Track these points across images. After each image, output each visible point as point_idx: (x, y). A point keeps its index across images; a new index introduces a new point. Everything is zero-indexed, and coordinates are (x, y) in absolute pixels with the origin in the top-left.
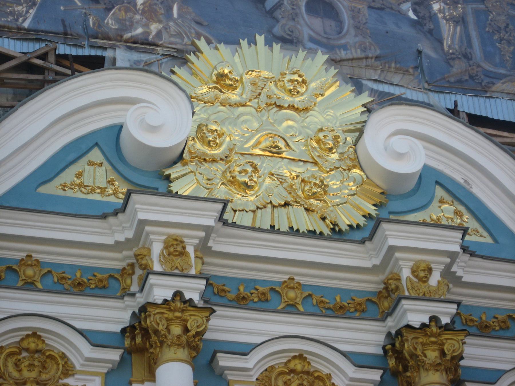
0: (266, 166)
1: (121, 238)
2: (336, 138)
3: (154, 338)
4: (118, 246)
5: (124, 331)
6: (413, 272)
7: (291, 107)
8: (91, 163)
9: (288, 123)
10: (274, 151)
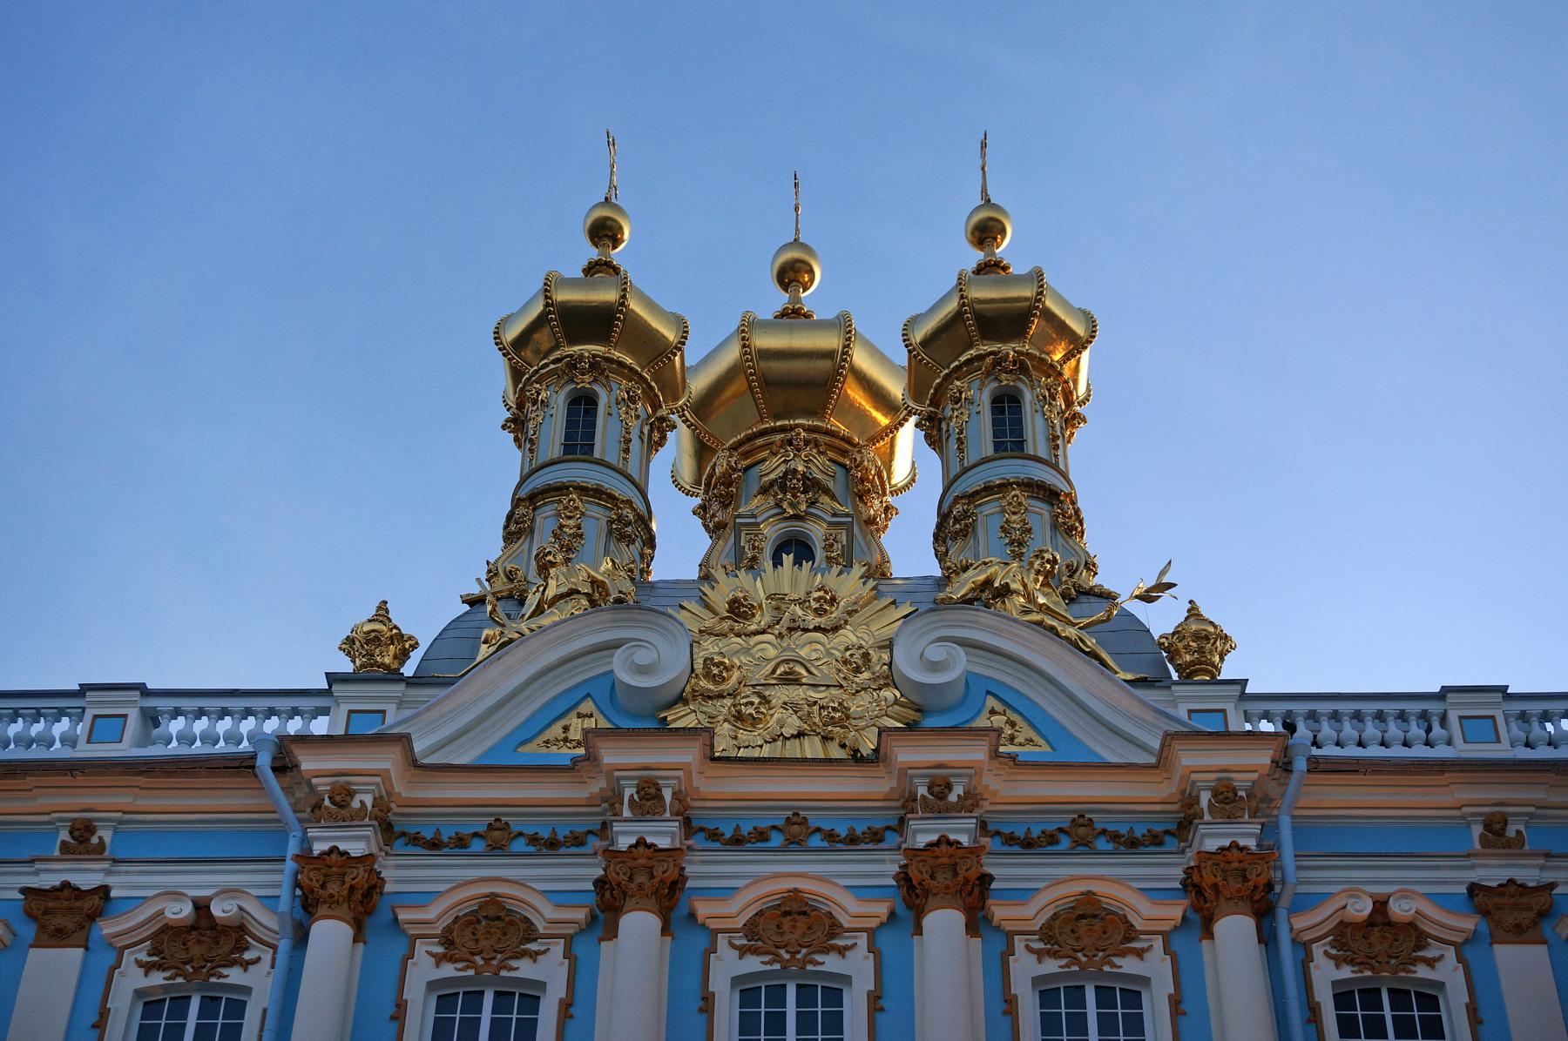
0: (780, 694)
2: (866, 656)
6: (930, 789)
7: (817, 629)
8: (580, 716)
9: (808, 648)
10: (790, 679)
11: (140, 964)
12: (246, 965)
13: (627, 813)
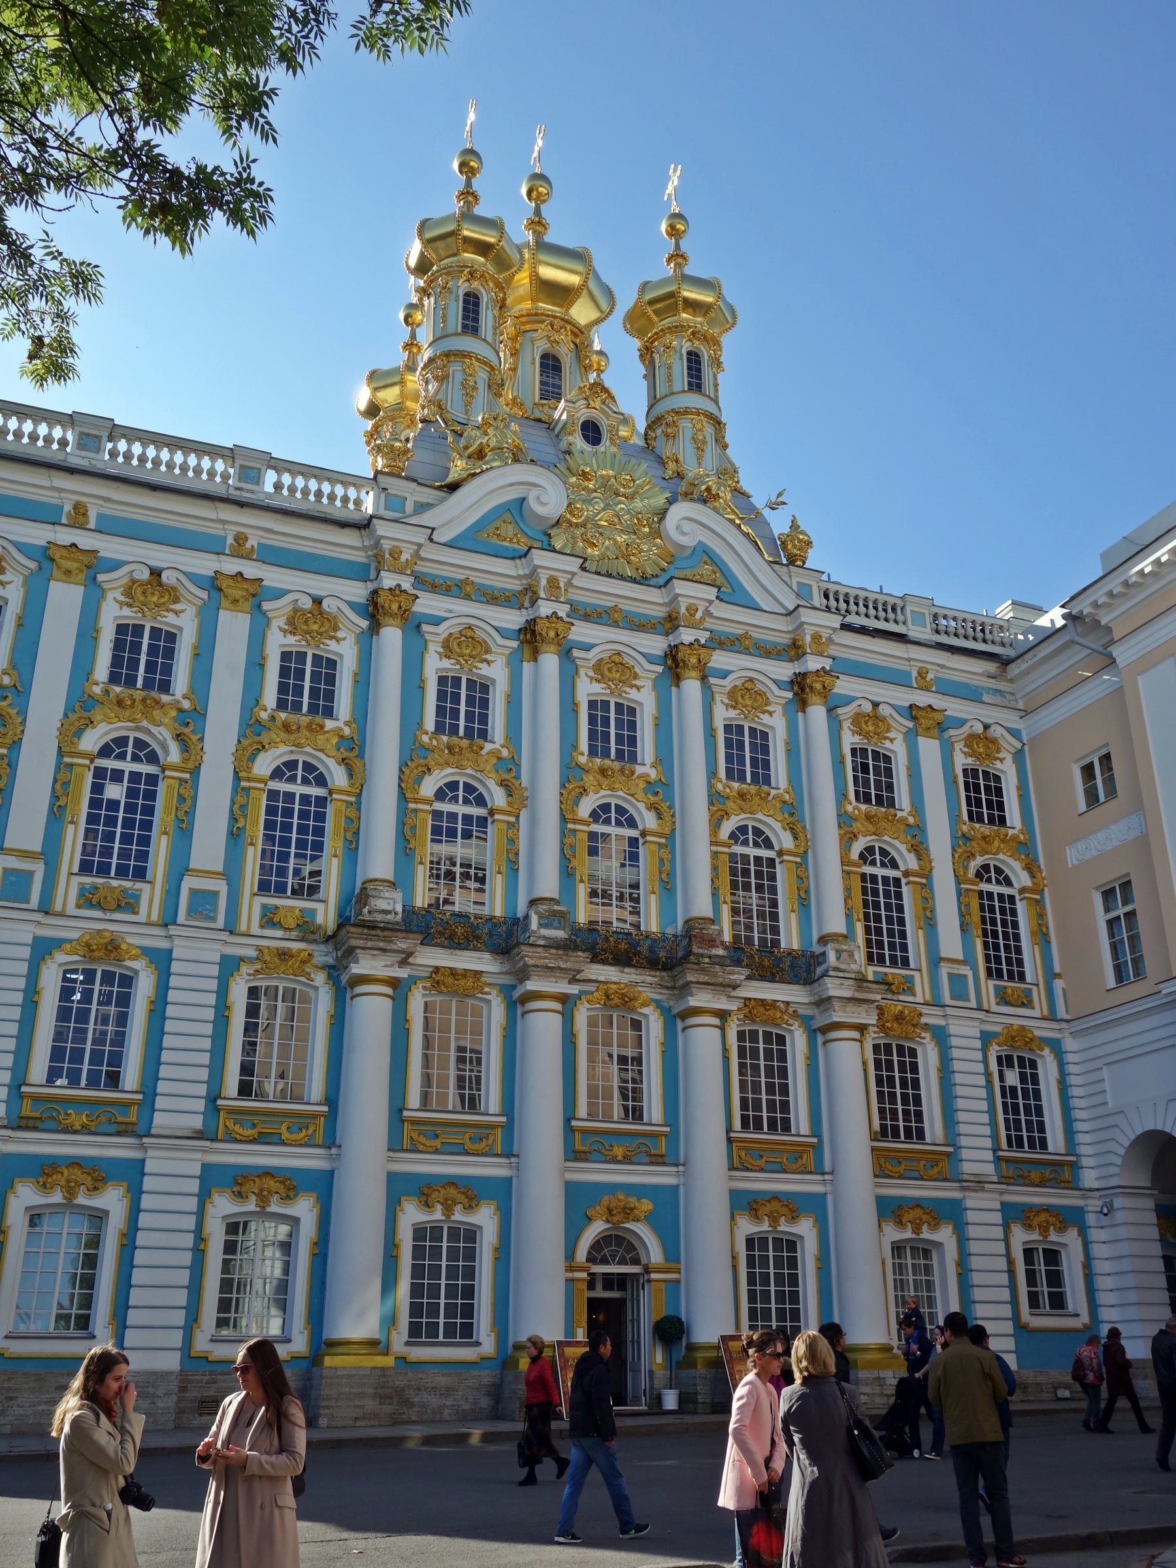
1: (521, 572)
3: (538, 638)
4: (519, 577)
5: (520, 630)
8: (504, 522)
11: (280, 629)
12: (338, 640)
13: (542, 595)
